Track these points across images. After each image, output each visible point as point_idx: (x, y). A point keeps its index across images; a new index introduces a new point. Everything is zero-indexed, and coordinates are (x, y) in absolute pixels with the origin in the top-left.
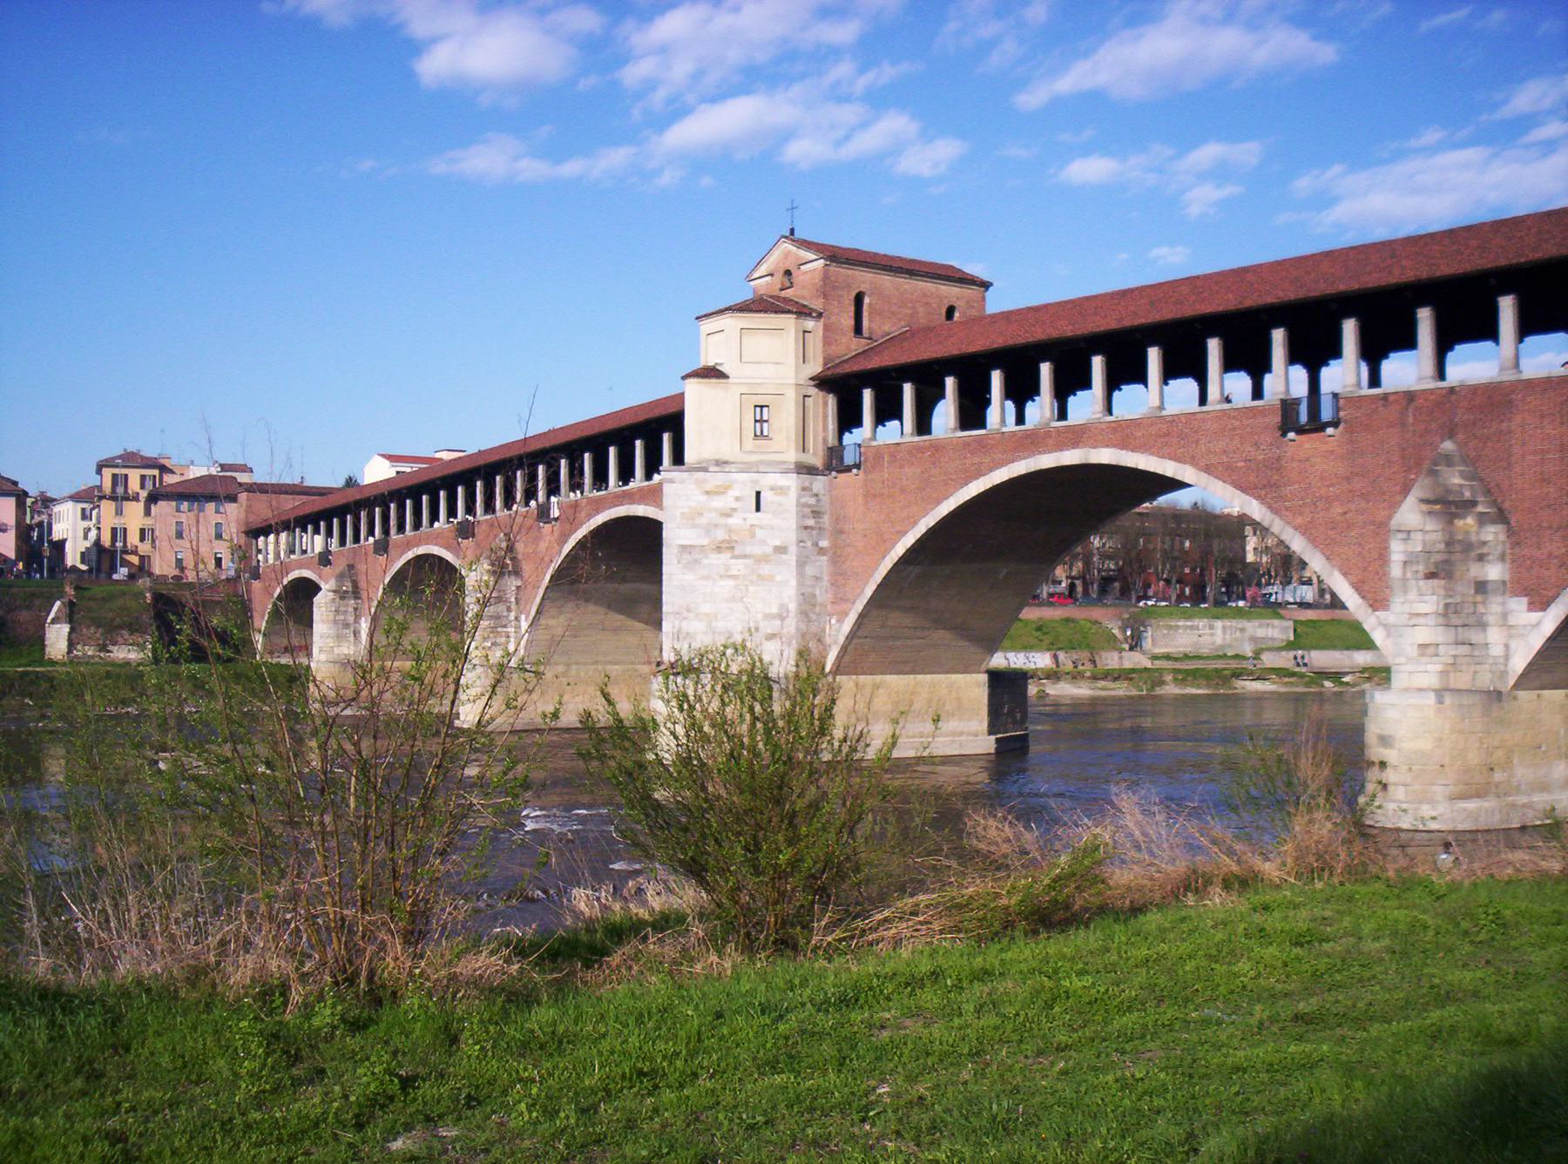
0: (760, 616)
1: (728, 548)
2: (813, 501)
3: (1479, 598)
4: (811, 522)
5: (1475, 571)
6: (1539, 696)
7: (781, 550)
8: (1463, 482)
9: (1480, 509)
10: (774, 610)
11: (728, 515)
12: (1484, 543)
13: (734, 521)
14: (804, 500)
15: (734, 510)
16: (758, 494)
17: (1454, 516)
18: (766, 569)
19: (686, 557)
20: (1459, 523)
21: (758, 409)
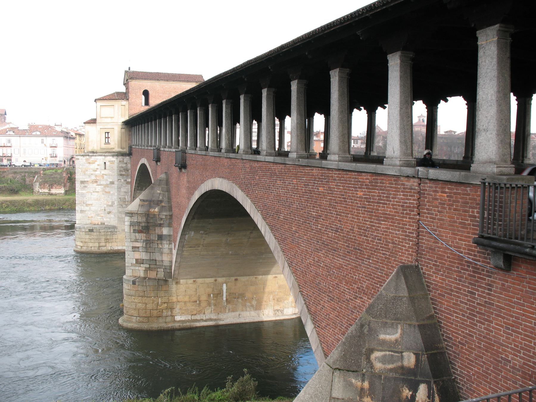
0: (105, 206)
1: (95, 182)
2: (124, 165)
3: (159, 242)
4: (124, 173)
5: (158, 231)
6: (194, 281)
7: (112, 183)
8: (161, 192)
9: (163, 204)
10: (110, 204)
11: (96, 171)
12: (162, 219)
13: (98, 173)
14: (120, 165)
15: (97, 169)
16: (105, 163)
17: (150, 207)
18: (107, 190)
19: (83, 185)
20: (152, 210)
21: (107, 134)
